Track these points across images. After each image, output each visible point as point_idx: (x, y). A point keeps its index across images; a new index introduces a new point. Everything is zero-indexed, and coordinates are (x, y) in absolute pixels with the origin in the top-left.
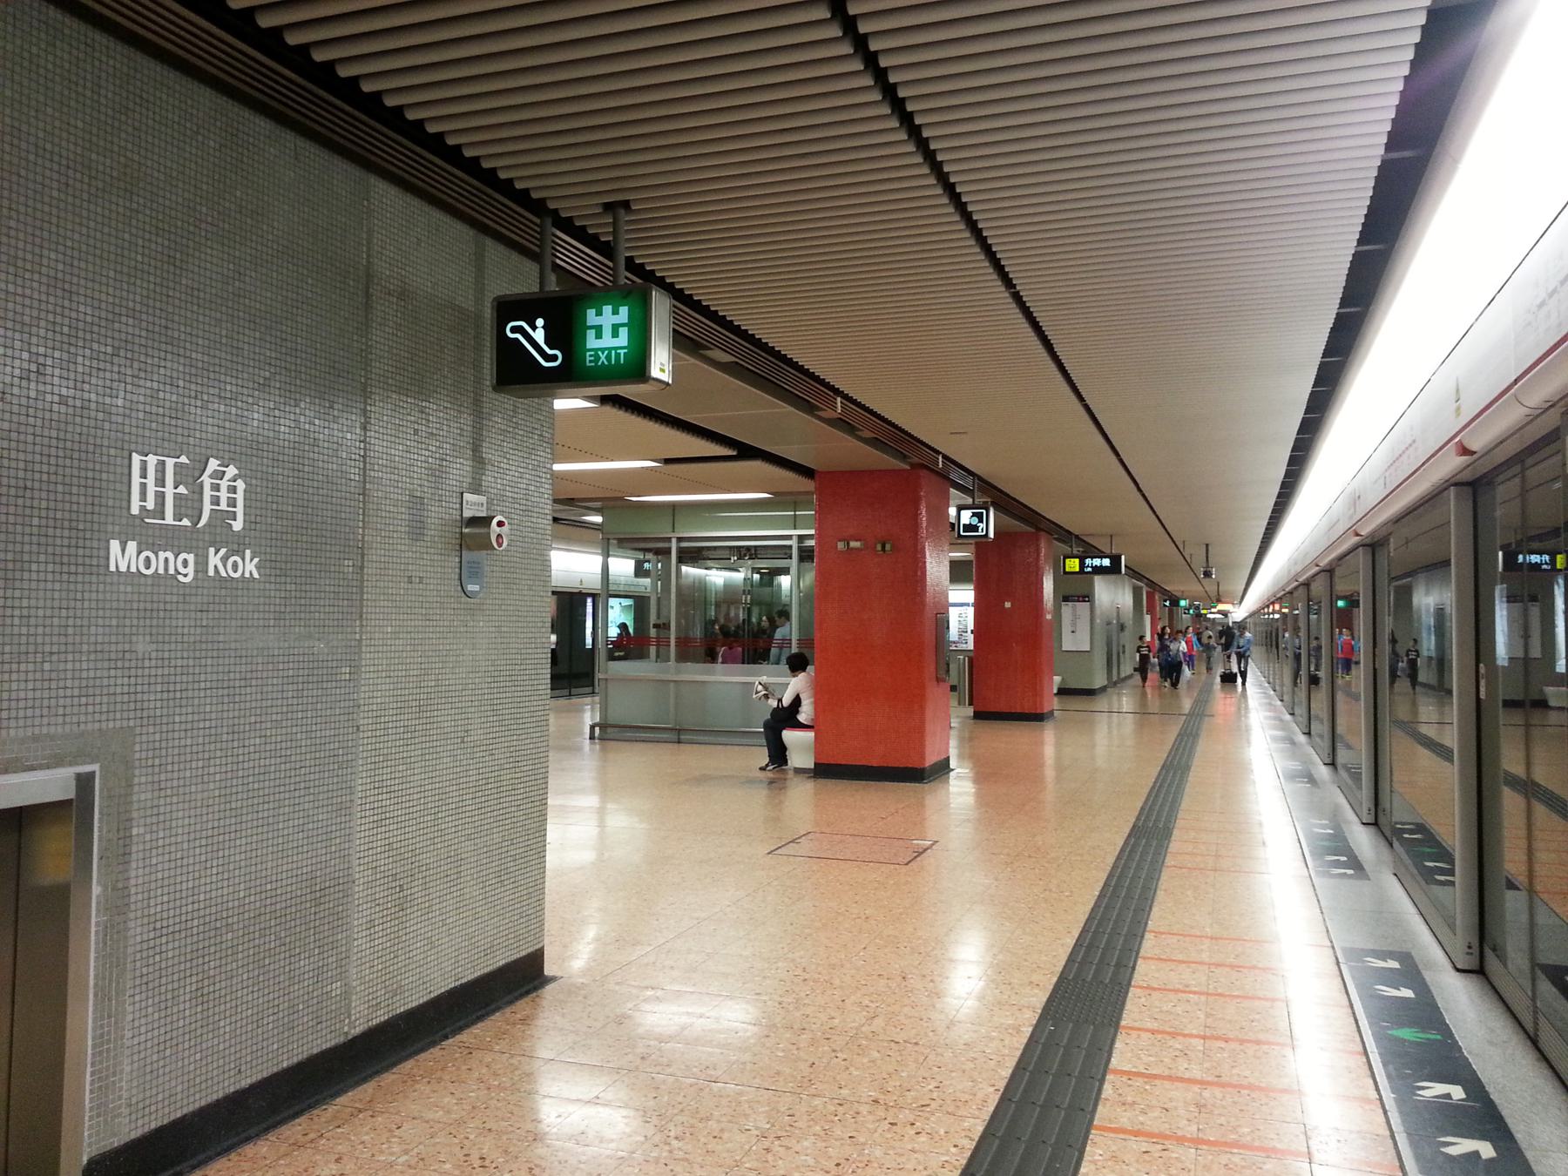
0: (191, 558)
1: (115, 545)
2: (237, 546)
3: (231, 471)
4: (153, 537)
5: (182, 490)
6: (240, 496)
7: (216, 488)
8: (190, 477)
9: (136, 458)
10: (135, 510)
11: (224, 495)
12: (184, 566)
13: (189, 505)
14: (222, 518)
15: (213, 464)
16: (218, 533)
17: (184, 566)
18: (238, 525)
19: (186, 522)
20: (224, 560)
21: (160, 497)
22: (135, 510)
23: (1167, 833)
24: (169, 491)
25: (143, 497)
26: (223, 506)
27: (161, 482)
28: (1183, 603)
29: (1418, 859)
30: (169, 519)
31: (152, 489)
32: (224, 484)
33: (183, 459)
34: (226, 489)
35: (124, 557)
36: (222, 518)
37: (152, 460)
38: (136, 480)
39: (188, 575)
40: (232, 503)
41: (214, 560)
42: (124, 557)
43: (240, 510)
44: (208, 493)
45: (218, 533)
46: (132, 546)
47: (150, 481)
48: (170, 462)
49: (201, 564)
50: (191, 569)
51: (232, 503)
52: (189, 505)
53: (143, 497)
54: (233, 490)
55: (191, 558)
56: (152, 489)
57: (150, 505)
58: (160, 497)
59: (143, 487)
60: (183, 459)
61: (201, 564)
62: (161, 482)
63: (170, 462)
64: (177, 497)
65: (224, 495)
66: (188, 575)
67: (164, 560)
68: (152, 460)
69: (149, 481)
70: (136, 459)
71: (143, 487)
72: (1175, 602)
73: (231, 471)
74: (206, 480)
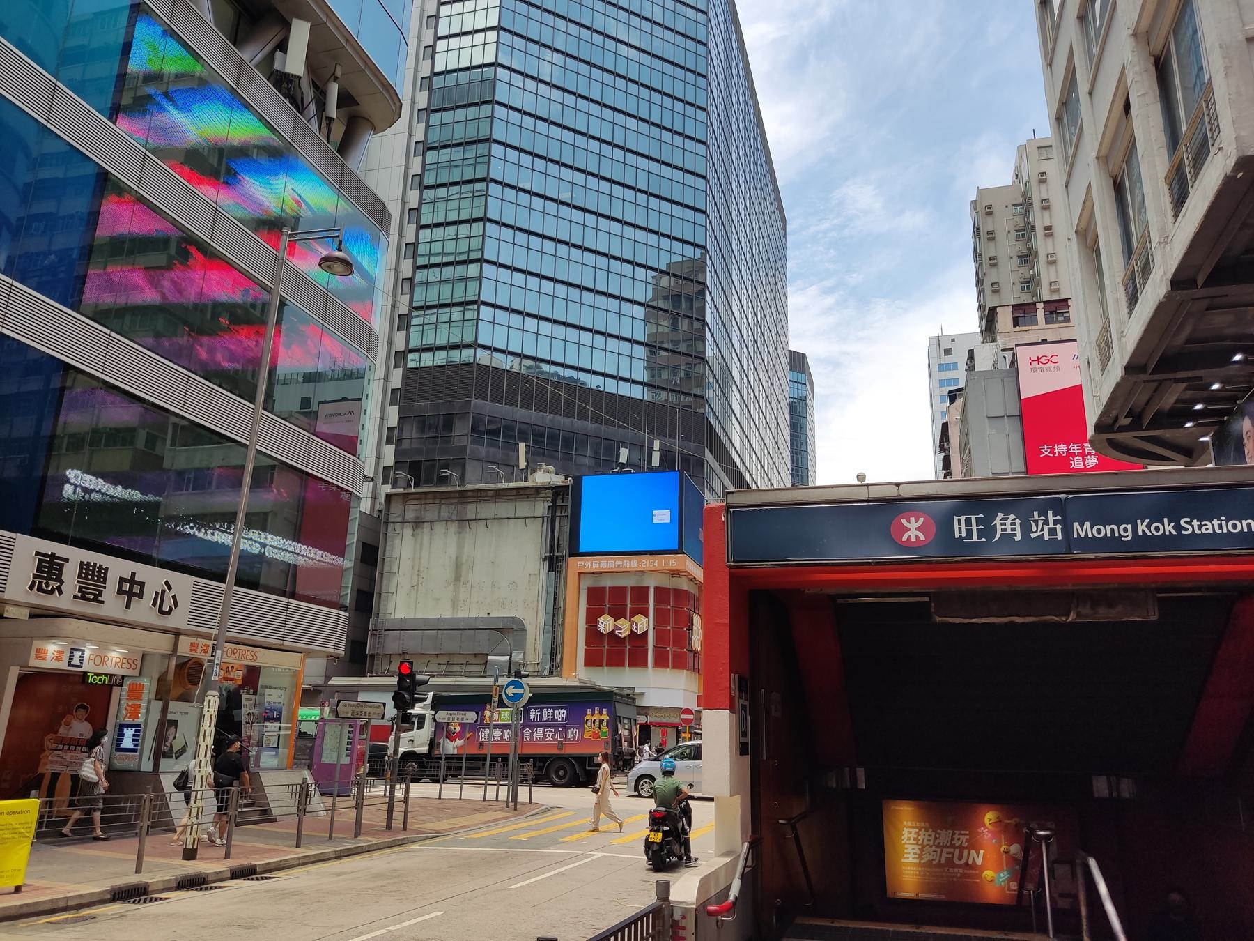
3: (1012, 516)
6: (1018, 527)
11: (1008, 527)
21: (969, 533)
24: (974, 528)
26: (1009, 531)
37: (963, 518)
40: (1014, 529)
43: (1018, 532)
44: (999, 528)
48: (973, 518)
51: (1014, 529)
57: (964, 534)
58: (969, 533)
65: (1008, 527)
68: (963, 518)
70: (956, 518)
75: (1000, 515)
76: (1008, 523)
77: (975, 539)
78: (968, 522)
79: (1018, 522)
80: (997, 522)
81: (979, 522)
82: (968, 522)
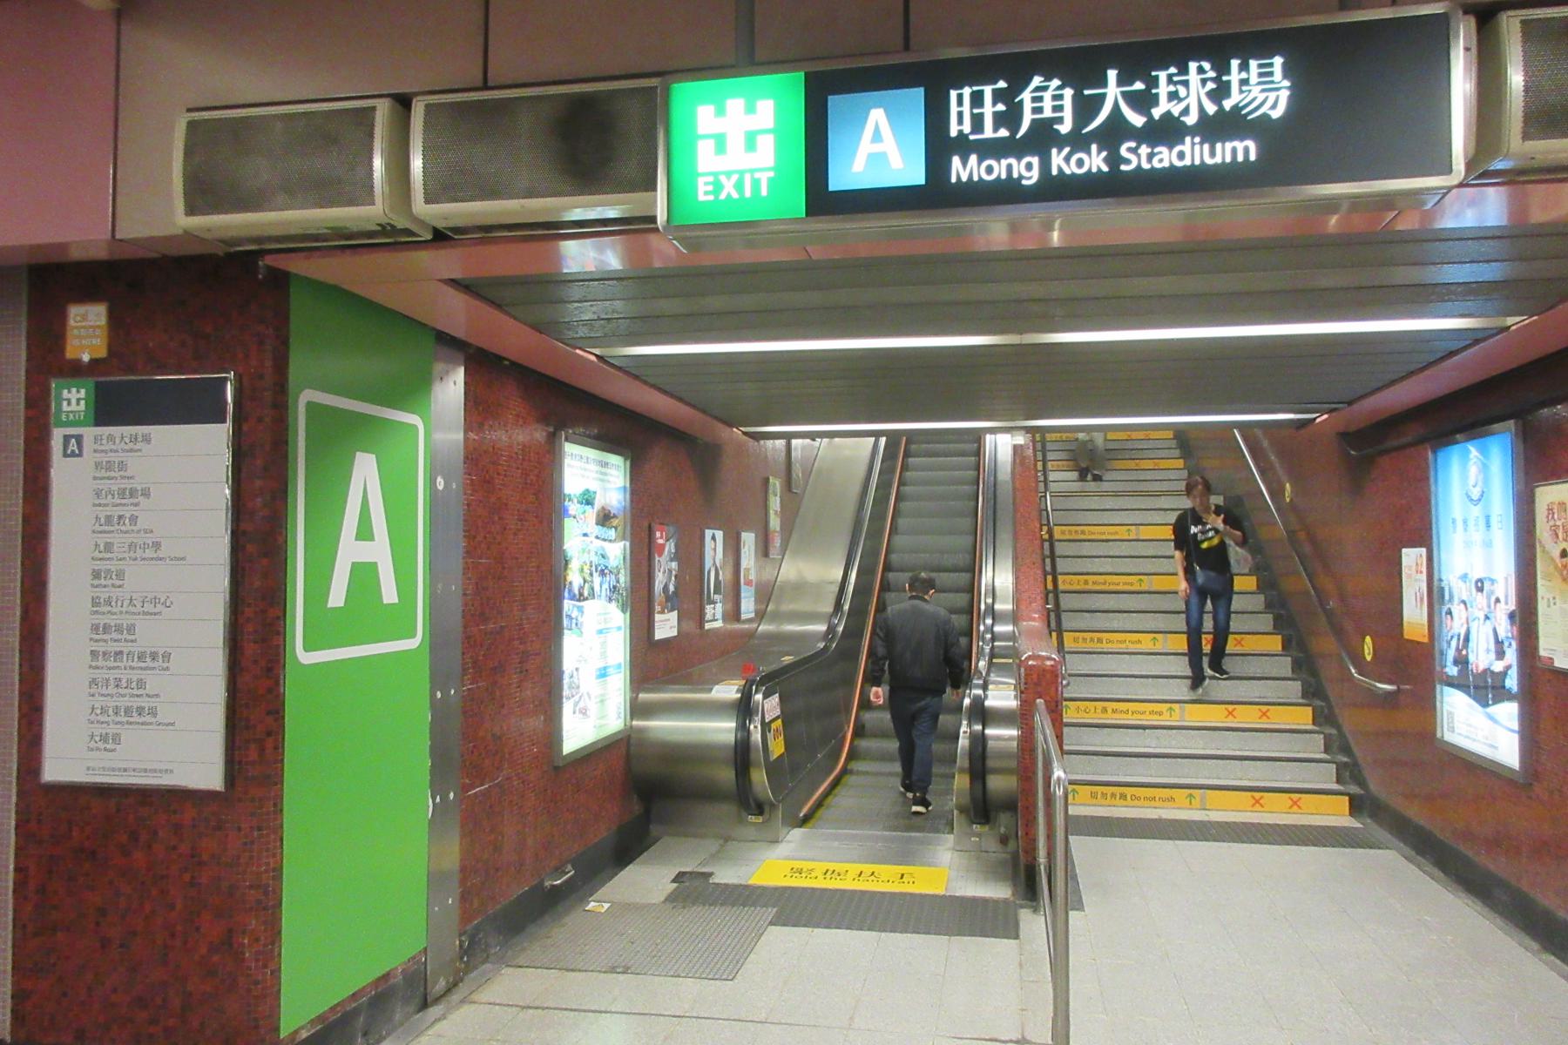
3: (1056, 82)
5: (1001, 107)
11: (1048, 104)
19: (1003, 133)
24: (988, 110)
25: (960, 122)
33: (1002, 84)
37: (967, 91)
44: (1028, 106)
48: (988, 90)
52: (1010, 118)
53: (960, 122)
57: (967, 128)
59: (960, 115)
60: (1002, 84)
64: (996, 115)
65: (1048, 104)
70: (953, 94)
71: (960, 115)
75: (1037, 81)
76: (1047, 95)
77: (988, 132)
78: (977, 99)
79: (1068, 93)
80: (1026, 96)
81: (998, 96)
82: (977, 99)
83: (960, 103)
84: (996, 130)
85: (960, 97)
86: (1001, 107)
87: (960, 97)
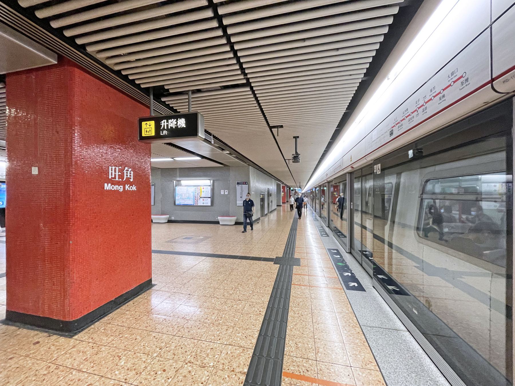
0: (122, 187)
1: (106, 184)
2: (131, 184)
3: (130, 170)
4: (113, 183)
5: (120, 173)
6: (132, 175)
7: (127, 173)
8: (121, 171)
9: (110, 167)
10: (110, 178)
11: (129, 174)
12: (120, 188)
13: (121, 176)
14: (128, 179)
15: (126, 168)
16: (128, 181)
17: (120, 188)
18: (132, 180)
20: (129, 187)
21: (115, 175)
22: (110, 178)
23: (296, 230)
24: (117, 174)
25: (112, 175)
26: (129, 176)
27: (115, 172)
28: (292, 189)
29: (336, 233)
30: (117, 179)
31: (113, 173)
32: (129, 172)
34: (129, 173)
35: (108, 187)
36: (128, 179)
37: (113, 168)
38: (110, 172)
39: (121, 190)
40: (130, 176)
41: (127, 187)
42: (108, 187)
44: (125, 174)
45: (128, 181)
46: (110, 184)
47: (113, 172)
48: (117, 168)
49: (124, 188)
50: (122, 189)
51: (130, 176)
52: (121, 176)
53: (112, 175)
54: (130, 173)
55: (122, 187)
56: (113, 173)
57: (113, 176)
58: (115, 175)
59: (112, 173)
61: (124, 188)
62: (115, 172)
63: (117, 168)
64: (119, 175)
65: (129, 174)
66: (121, 190)
67: (116, 187)
68: (113, 168)
69: (113, 172)
71: (112, 173)
72: (290, 189)
73: (130, 170)
74: (125, 171)
76: (129, 172)
77: (117, 179)
79: (132, 172)
83: (112, 170)
84: (119, 178)
85: (112, 169)
86: (120, 173)
87: (112, 169)
